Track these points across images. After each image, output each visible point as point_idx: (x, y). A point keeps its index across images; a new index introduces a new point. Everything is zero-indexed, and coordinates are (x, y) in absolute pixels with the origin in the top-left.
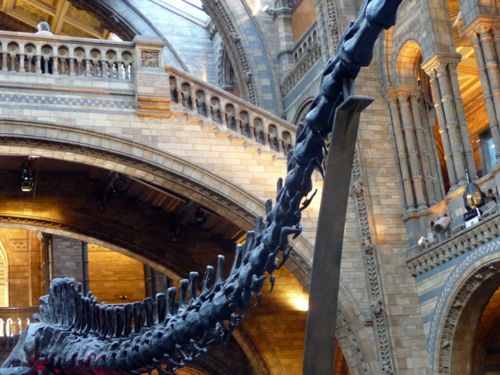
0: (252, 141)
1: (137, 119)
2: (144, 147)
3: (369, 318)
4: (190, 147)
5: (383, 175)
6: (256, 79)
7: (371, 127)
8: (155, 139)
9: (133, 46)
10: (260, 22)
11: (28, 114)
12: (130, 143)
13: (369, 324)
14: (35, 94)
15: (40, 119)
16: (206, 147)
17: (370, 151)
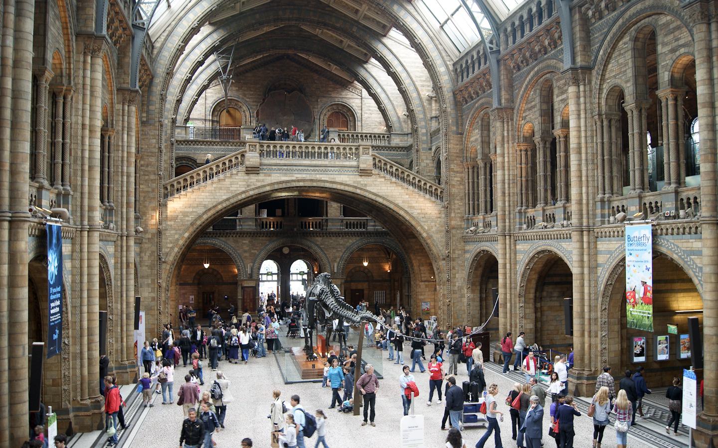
0: (405, 185)
1: (359, 177)
2: (361, 189)
3: (444, 257)
4: (379, 188)
5: (458, 200)
6: (419, 129)
7: (456, 179)
8: (366, 185)
9: (359, 146)
10: (424, 100)
11: (318, 177)
12: (356, 187)
13: (444, 259)
14: (321, 168)
15: (323, 179)
16: (386, 188)
17: (454, 189)
